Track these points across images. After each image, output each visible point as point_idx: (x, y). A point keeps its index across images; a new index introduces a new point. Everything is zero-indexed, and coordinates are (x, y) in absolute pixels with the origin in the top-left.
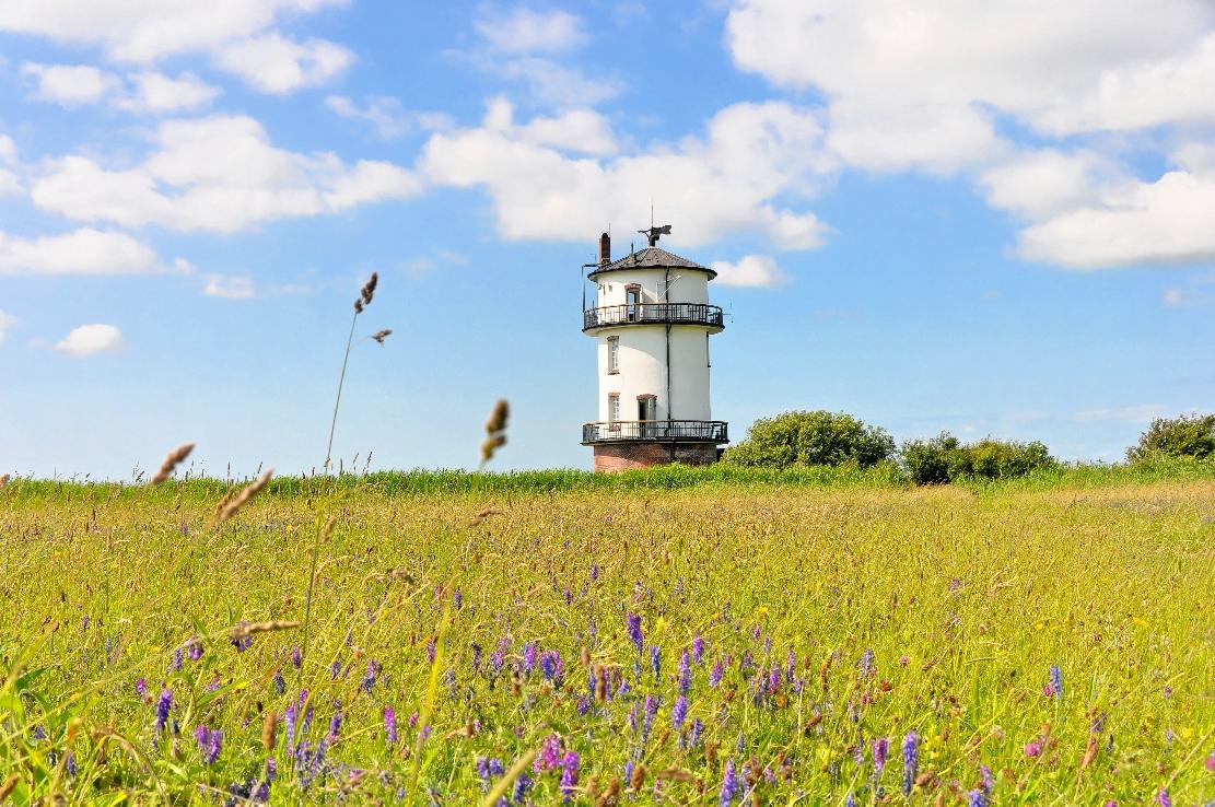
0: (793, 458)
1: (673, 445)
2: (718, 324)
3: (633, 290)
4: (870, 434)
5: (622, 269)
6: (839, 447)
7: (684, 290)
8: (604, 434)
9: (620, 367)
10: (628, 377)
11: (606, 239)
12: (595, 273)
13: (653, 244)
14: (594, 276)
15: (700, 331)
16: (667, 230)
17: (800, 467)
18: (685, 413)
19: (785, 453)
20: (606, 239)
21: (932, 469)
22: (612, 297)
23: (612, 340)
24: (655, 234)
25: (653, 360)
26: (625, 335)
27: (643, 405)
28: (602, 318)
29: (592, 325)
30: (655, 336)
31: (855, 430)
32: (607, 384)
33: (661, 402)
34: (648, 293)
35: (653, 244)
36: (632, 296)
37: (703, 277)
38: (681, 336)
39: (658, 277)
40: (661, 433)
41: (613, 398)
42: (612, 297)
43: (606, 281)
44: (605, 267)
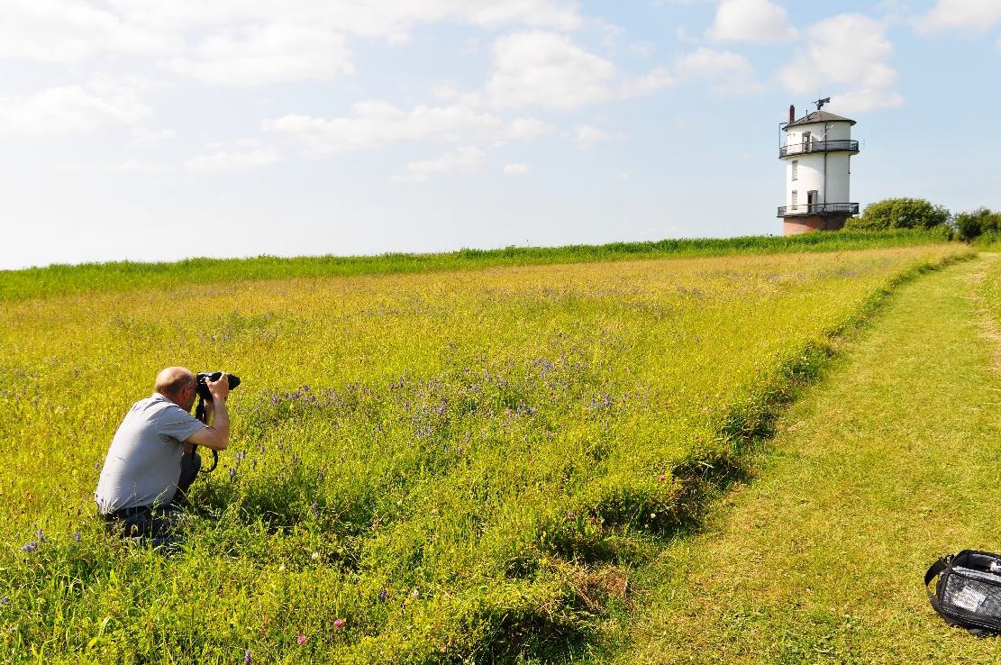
0: (888, 224)
1: (826, 219)
2: (855, 150)
3: (807, 135)
4: (935, 209)
5: (800, 125)
6: (915, 218)
7: (835, 133)
8: (789, 212)
9: (798, 177)
10: (802, 182)
11: (792, 109)
12: (787, 127)
13: (819, 109)
14: (786, 129)
15: (845, 155)
16: (828, 100)
17: (892, 231)
18: (833, 200)
19: (883, 222)
20: (792, 109)
21: (973, 229)
22: (795, 140)
23: (794, 162)
24: (821, 103)
25: (816, 172)
26: (799, 159)
27: (811, 196)
28: (788, 153)
29: (783, 155)
30: (819, 159)
31: (928, 207)
32: (791, 186)
33: (821, 194)
34: (816, 136)
35: (819, 109)
36: (806, 139)
37: (848, 124)
38: (832, 158)
39: (822, 127)
40: (819, 210)
41: (794, 193)
42: (795, 140)
43: (792, 131)
44: (792, 124)
